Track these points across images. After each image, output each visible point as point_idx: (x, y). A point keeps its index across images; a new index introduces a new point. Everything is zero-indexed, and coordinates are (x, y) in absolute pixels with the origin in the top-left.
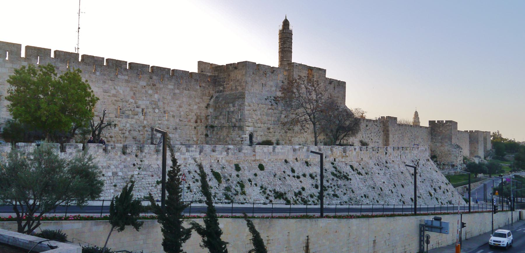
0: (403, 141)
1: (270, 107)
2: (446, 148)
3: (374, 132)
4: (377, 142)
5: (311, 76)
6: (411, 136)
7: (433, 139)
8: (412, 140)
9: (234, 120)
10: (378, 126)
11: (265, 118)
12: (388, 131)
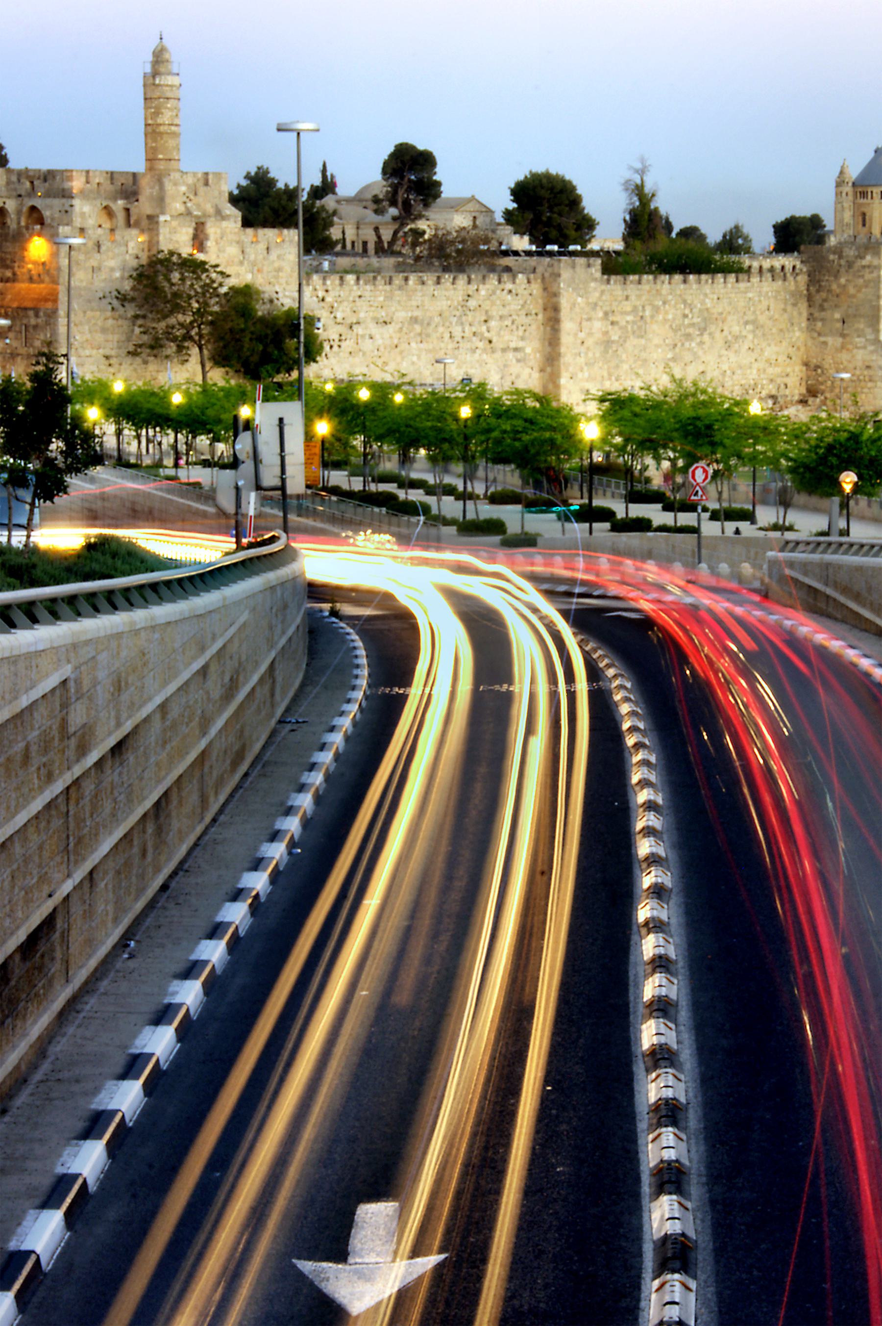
0: (642, 337)
1: (109, 314)
2: (860, 355)
3: (501, 317)
4: (516, 350)
5: (201, 236)
6: (685, 316)
7: (815, 320)
8: (691, 330)
9: (37, 343)
10: (520, 291)
11: (99, 337)
12: (556, 309)
